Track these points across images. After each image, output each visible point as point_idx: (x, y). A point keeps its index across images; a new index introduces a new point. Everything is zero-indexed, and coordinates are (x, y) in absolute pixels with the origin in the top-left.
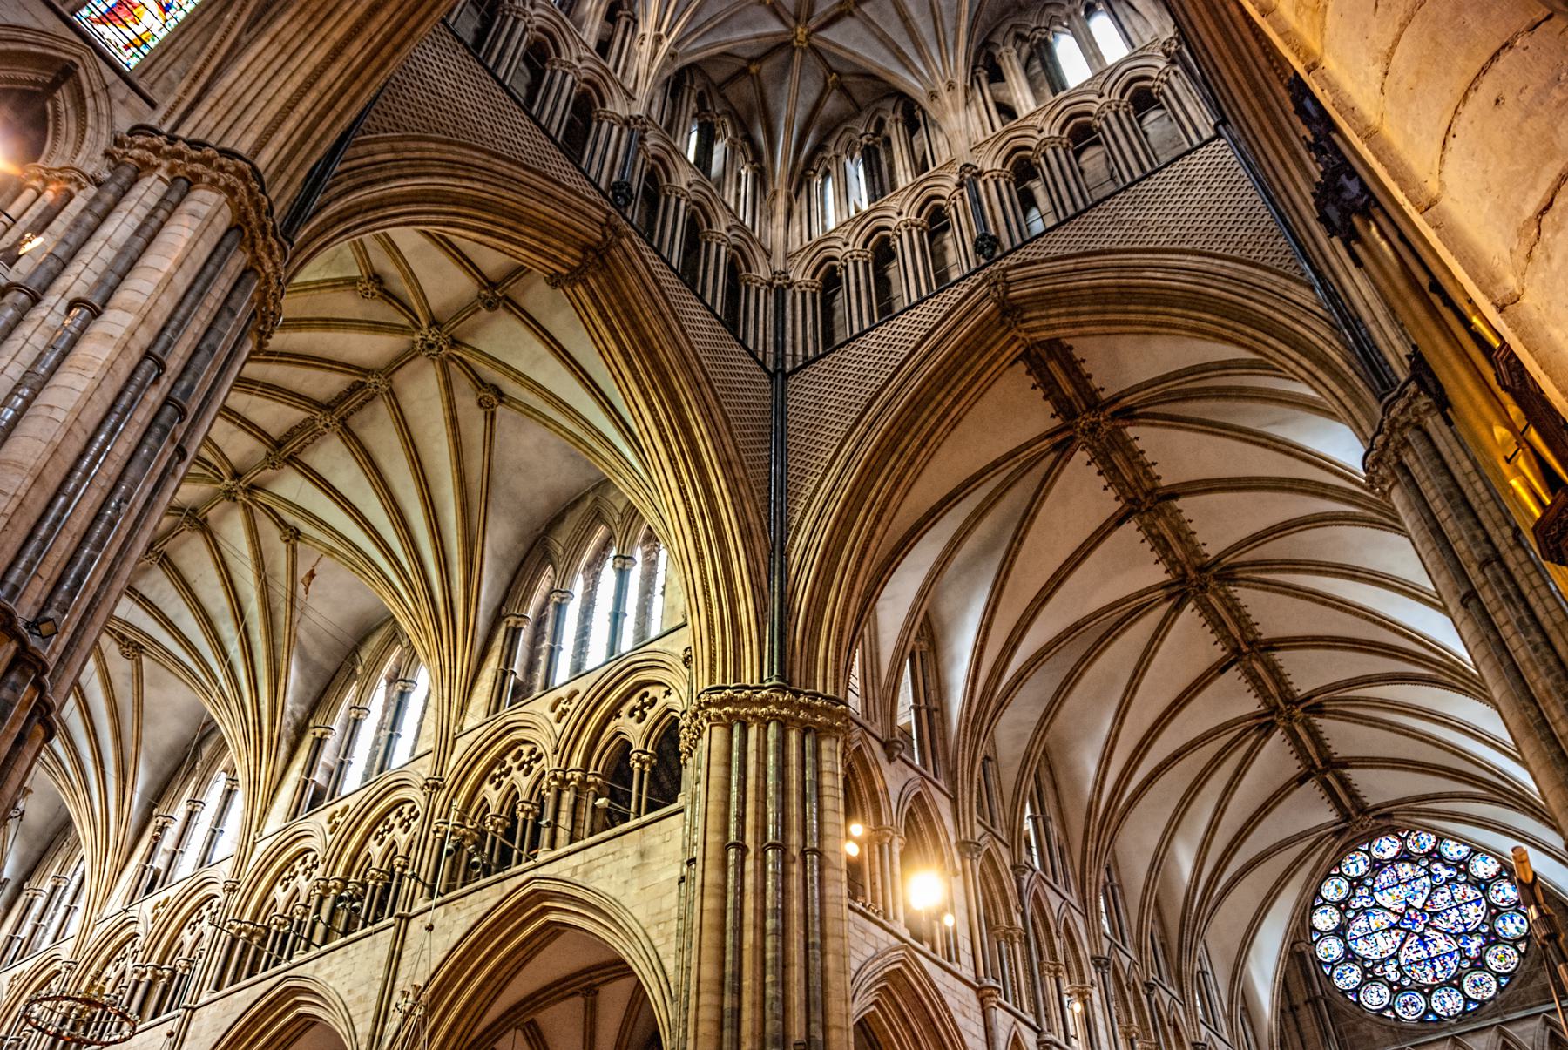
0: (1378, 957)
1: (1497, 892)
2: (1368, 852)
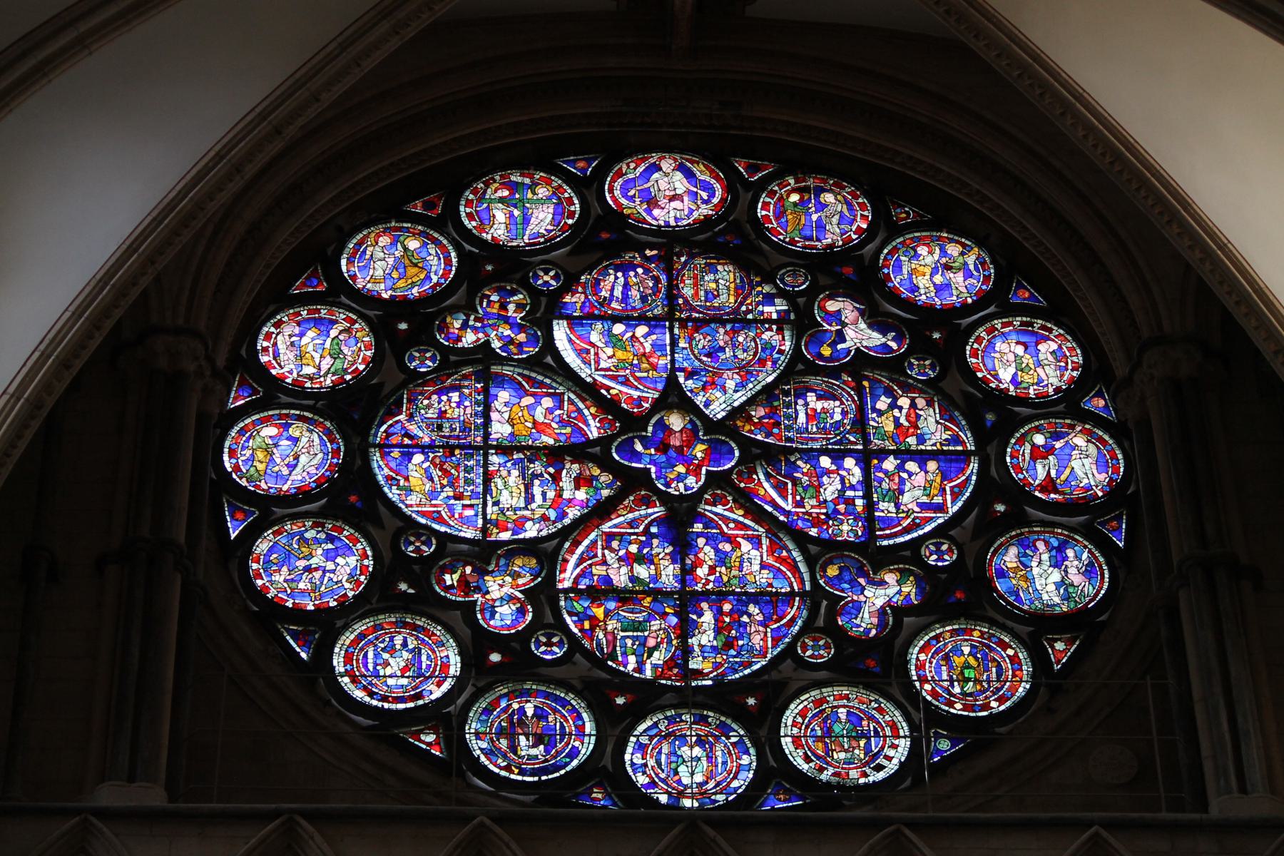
0: (469, 534)
1: (1039, 454)
2: (590, 187)
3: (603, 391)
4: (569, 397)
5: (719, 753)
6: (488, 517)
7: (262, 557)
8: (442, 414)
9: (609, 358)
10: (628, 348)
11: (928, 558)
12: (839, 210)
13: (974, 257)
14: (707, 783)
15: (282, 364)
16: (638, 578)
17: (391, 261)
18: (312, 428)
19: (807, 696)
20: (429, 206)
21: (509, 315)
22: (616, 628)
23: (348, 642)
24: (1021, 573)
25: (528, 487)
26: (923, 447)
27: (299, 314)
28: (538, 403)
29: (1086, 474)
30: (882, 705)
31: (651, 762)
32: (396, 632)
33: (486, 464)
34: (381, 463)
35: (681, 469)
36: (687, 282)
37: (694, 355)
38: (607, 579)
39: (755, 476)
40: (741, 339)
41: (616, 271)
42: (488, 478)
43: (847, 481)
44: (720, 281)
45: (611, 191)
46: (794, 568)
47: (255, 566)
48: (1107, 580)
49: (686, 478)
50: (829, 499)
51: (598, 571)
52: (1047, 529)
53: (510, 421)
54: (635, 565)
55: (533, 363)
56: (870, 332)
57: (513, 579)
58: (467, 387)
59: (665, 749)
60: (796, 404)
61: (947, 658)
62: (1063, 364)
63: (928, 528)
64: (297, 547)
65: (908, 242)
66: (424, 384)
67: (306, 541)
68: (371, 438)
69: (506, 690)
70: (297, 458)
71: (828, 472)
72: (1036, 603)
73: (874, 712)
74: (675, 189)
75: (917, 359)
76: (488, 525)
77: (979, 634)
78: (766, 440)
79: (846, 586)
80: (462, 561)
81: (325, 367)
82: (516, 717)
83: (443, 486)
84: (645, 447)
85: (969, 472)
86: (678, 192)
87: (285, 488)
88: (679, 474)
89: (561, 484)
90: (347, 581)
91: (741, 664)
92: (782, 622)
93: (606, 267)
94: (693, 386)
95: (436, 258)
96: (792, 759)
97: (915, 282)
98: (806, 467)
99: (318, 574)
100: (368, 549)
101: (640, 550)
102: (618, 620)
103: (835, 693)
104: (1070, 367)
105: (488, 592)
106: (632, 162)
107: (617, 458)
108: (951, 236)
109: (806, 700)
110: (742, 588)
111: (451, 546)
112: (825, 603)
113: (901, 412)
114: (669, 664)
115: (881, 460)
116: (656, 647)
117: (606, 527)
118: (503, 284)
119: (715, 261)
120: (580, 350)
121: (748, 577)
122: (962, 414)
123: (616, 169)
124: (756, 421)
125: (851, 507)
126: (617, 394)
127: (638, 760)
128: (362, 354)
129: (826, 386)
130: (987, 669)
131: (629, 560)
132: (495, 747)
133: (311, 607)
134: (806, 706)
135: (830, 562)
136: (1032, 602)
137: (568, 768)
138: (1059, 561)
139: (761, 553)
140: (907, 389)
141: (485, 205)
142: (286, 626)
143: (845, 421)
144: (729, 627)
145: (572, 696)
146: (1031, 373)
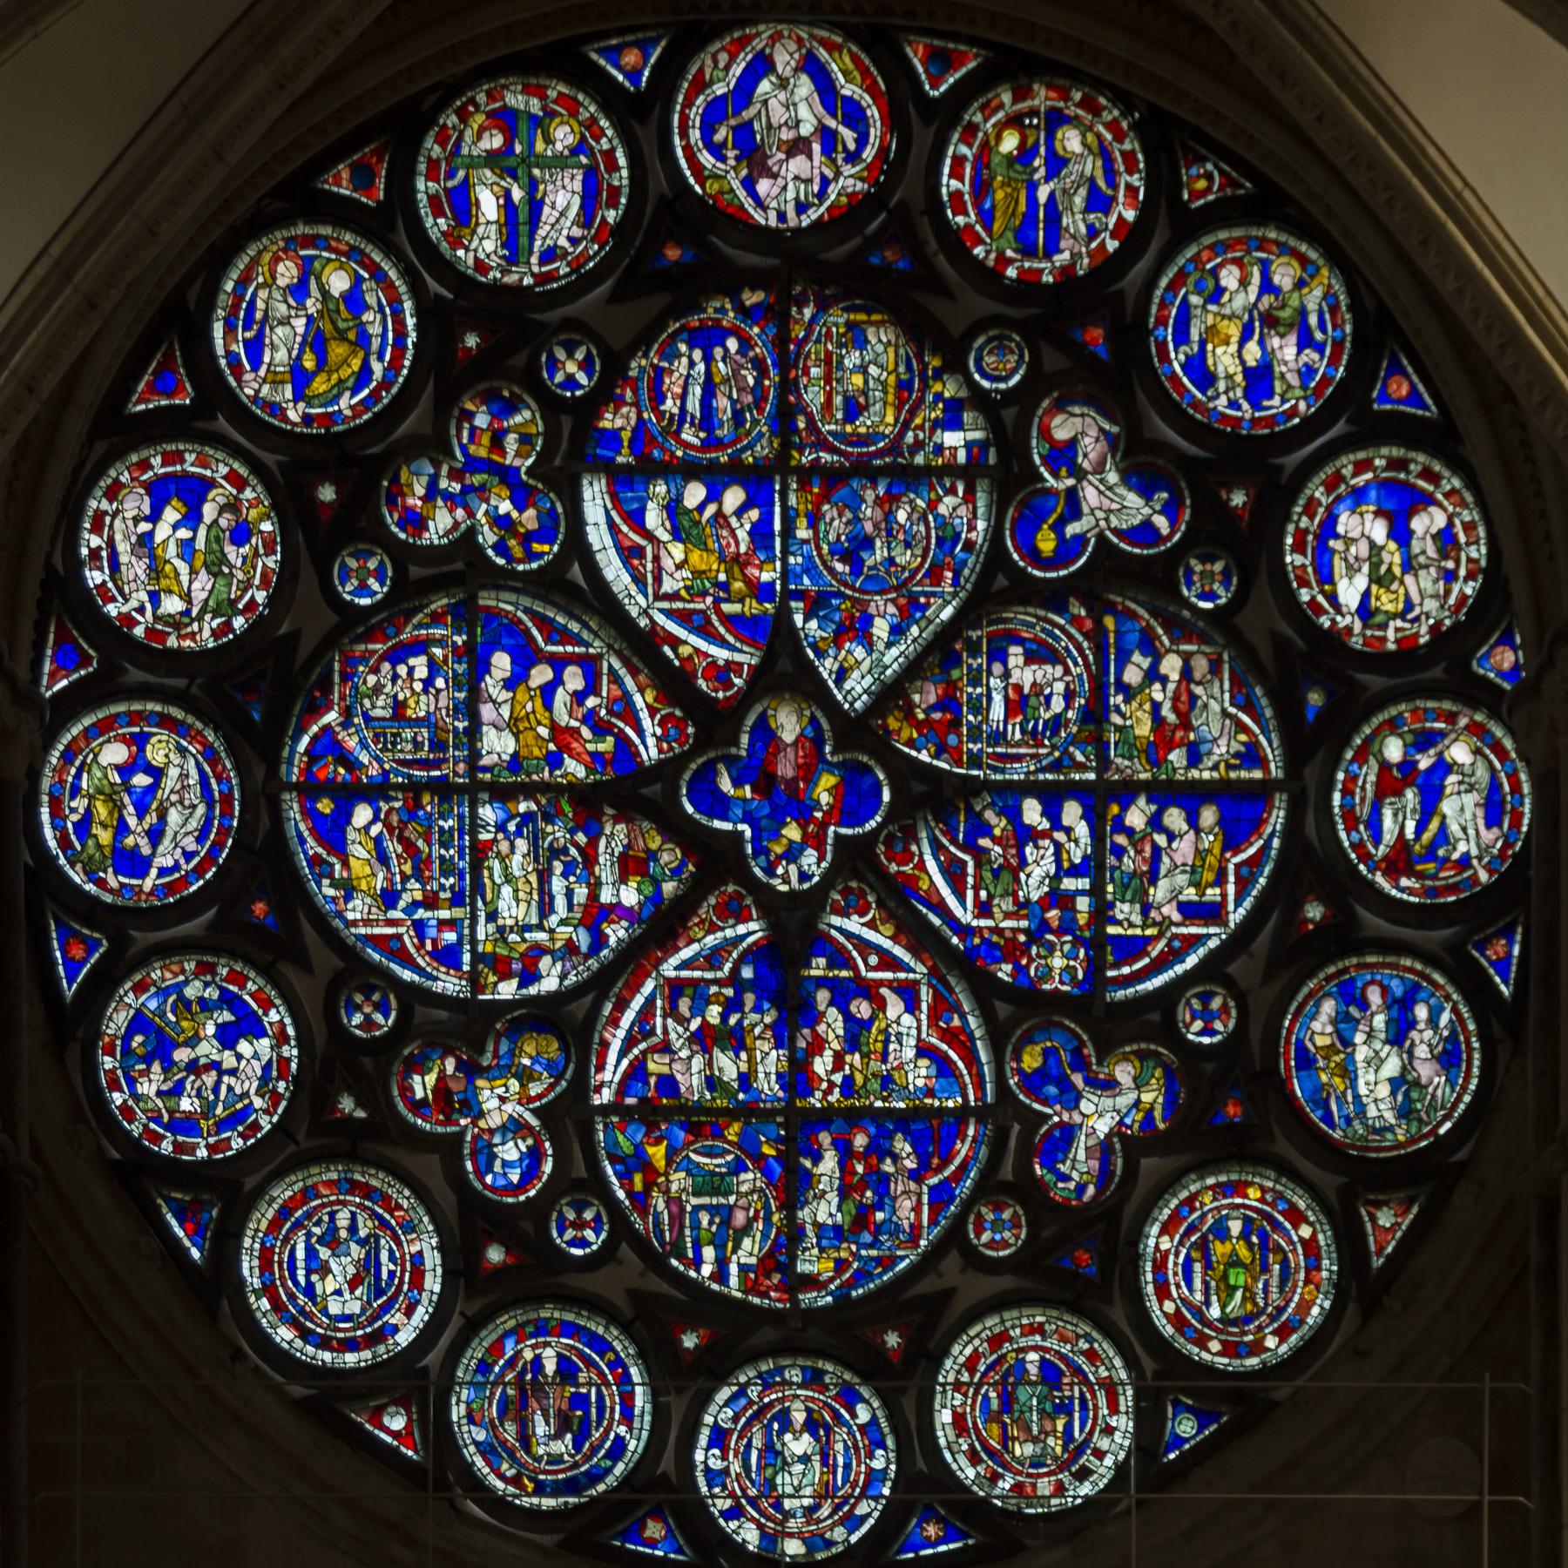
0: (449, 984)
1: (1391, 782)
3: (667, 650)
4: (610, 666)
5: (839, 1447)
6: (480, 948)
7: (119, 1042)
8: (399, 707)
9: (679, 567)
10: (710, 542)
11: (1187, 1026)
12: (1088, 172)
13: (1318, 292)
14: (817, 1507)
15: (127, 590)
16: (720, 1079)
17: (300, 324)
18: (185, 744)
19: (978, 1328)
20: (363, 177)
21: (508, 462)
22: (684, 1189)
23: (264, 1225)
24: (1337, 1059)
25: (544, 876)
26: (1195, 773)
27: (145, 465)
28: (558, 681)
29: (1464, 829)
30: (1096, 1345)
31: (736, 1467)
32: (339, 1202)
33: (476, 825)
34: (302, 827)
35: (792, 832)
36: (814, 371)
37: (820, 555)
38: (668, 1084)
39: (914, 848)
40: (902, 516)
41: (691, 347)
42: (480, 852)
43: (1065, 856)
44: (873, 370)
45: (684, 134)
46: (971, 1058)
47: (108, 1062)
48: (1476, 1071)
49: (801, 851)
50: (1035, 896)
51: (657, 1065)
52: (1389, 959)
53: (514, 725)
54: (717, 1052)
55: (549, 584)
56: (1122, 490)
57: (522, 1086)
58: (441, 642)
59: (757, 1442)
60: (990, 673)
61: (1203, 1246)
62: (1450, 565)
63: (1191, 961)
64: (173, 1019)
65: (1205, 255)
66: (369, 637)
67: (187, 1004)
68: (284, 768)
69: (512, 1323)
70: (162, 817)
71: (1031, 834)
72: (1356, 1124)
73: (1081, 1360)
74: (798, 122)
75: (1203, 562)
76: (481, 966)
77: (1258, 1194)
78: (935, 762)
79: (1052, 1090)
80: (440, 1045)
81: (199, 596)
82: (529, 1377)
83: (405, 878)
84: (737, 783)
85: (1269, 830)
86: (806, 130)
87: (148, 884)
88: (791, 841)
89: (597, 869)
90: (258, 1093)
91: (878, 1261)
92: (947, 1173)
93: (674, 337)
94: (820, 633)
95: (378, 317)
96: (948, 1456)
97: (1210, 362)
98: (999, 825)
99: (209, 1079)
100: (287, 1021)
101: (724, 1017)
102: (689, 1173)
103: (1025, 1321)
104: (1462, 572)
105: (481, 1114)
106: (723, 49)
107: (690, 809)
108: (1283, 238)
109: (978, 1335)
110: (884, 1100)
111: (420, 1011)
112: (1017, 1127)
113: (1164, 690)
114: (768, 1263)
115: (1125, 808)
116: (746, 1230)
117: (669, 969)
118: (495, 384)
119: (861, 317)
120: (629, 549)
121: (896, 1075)
122: (1268, 693)
123: (694, 70)
124: (921, 716)
125: (1069, 915)
126: (690, 657)
127: (717, 1464)
128: (260, 564)
129: (1043, 630)
130: (1265, 1268)
131: (704, 1040)
132: (496, 1437)
133: (202, 1153)
134: (976, 1350)
135: (1028, 1039)
136: (1348, 1121)
137: (610, 1480)
138: (1399, 1034)
139: (919, 1021)
140: (1181, 630)
141: (461, 174)
142: (165, 1192)
143: (1070, 714)
144: (863, 1185)
145: (616, 1333)
146: (1394, 586)
